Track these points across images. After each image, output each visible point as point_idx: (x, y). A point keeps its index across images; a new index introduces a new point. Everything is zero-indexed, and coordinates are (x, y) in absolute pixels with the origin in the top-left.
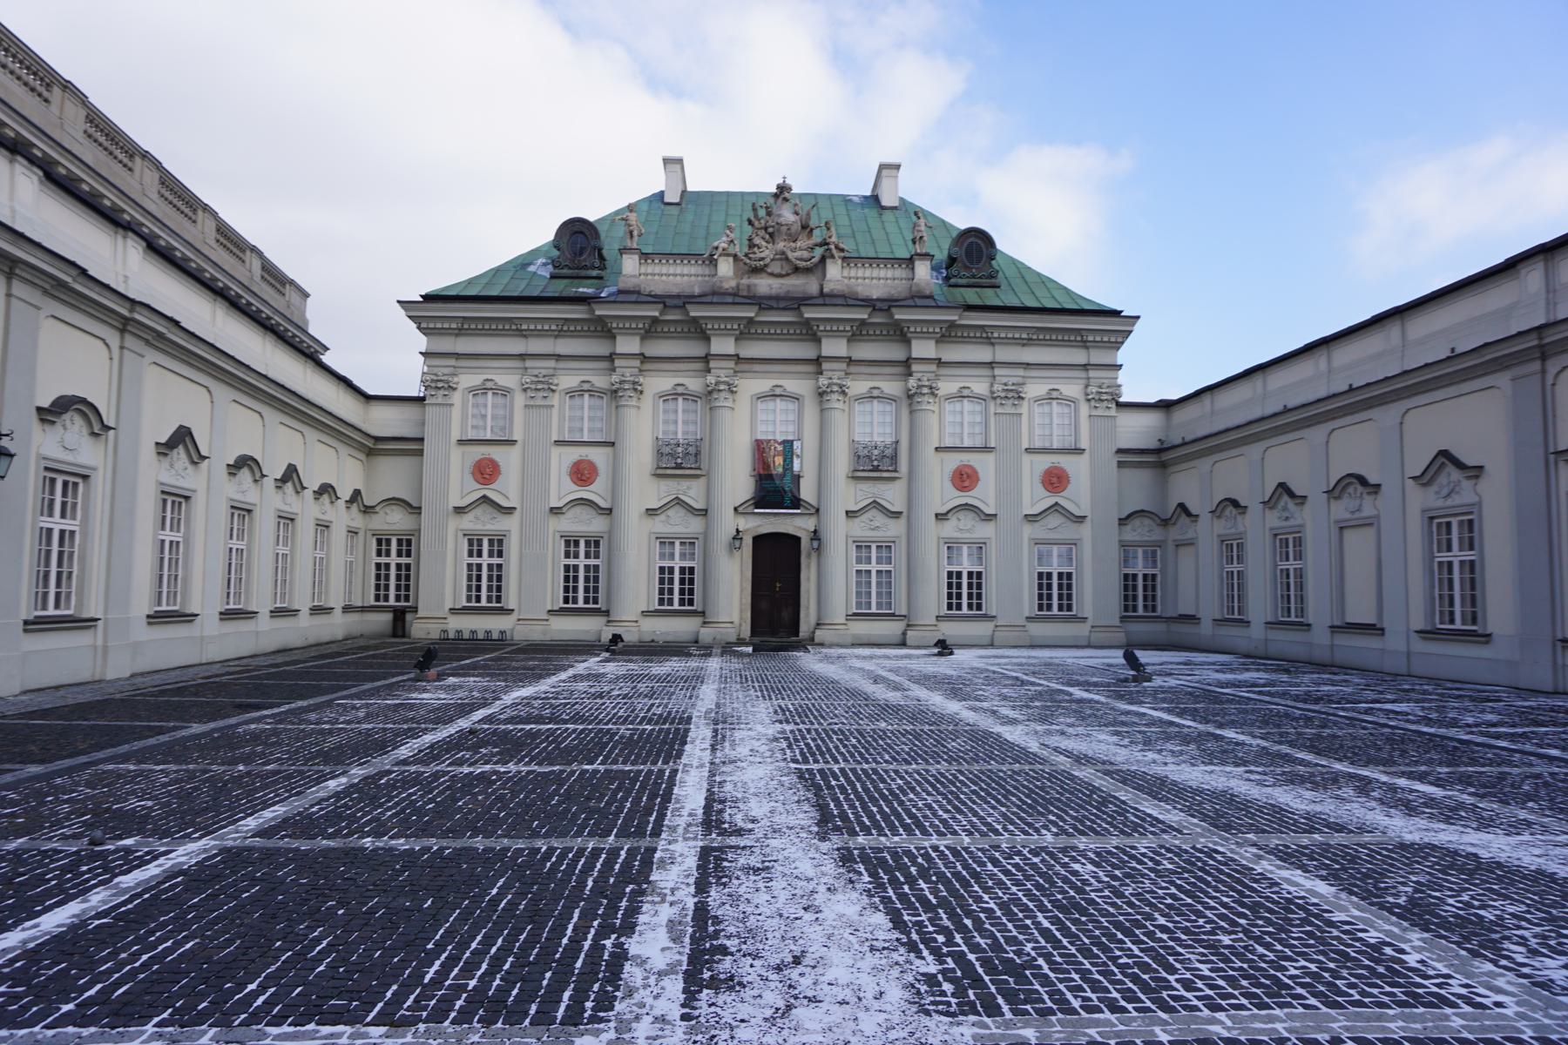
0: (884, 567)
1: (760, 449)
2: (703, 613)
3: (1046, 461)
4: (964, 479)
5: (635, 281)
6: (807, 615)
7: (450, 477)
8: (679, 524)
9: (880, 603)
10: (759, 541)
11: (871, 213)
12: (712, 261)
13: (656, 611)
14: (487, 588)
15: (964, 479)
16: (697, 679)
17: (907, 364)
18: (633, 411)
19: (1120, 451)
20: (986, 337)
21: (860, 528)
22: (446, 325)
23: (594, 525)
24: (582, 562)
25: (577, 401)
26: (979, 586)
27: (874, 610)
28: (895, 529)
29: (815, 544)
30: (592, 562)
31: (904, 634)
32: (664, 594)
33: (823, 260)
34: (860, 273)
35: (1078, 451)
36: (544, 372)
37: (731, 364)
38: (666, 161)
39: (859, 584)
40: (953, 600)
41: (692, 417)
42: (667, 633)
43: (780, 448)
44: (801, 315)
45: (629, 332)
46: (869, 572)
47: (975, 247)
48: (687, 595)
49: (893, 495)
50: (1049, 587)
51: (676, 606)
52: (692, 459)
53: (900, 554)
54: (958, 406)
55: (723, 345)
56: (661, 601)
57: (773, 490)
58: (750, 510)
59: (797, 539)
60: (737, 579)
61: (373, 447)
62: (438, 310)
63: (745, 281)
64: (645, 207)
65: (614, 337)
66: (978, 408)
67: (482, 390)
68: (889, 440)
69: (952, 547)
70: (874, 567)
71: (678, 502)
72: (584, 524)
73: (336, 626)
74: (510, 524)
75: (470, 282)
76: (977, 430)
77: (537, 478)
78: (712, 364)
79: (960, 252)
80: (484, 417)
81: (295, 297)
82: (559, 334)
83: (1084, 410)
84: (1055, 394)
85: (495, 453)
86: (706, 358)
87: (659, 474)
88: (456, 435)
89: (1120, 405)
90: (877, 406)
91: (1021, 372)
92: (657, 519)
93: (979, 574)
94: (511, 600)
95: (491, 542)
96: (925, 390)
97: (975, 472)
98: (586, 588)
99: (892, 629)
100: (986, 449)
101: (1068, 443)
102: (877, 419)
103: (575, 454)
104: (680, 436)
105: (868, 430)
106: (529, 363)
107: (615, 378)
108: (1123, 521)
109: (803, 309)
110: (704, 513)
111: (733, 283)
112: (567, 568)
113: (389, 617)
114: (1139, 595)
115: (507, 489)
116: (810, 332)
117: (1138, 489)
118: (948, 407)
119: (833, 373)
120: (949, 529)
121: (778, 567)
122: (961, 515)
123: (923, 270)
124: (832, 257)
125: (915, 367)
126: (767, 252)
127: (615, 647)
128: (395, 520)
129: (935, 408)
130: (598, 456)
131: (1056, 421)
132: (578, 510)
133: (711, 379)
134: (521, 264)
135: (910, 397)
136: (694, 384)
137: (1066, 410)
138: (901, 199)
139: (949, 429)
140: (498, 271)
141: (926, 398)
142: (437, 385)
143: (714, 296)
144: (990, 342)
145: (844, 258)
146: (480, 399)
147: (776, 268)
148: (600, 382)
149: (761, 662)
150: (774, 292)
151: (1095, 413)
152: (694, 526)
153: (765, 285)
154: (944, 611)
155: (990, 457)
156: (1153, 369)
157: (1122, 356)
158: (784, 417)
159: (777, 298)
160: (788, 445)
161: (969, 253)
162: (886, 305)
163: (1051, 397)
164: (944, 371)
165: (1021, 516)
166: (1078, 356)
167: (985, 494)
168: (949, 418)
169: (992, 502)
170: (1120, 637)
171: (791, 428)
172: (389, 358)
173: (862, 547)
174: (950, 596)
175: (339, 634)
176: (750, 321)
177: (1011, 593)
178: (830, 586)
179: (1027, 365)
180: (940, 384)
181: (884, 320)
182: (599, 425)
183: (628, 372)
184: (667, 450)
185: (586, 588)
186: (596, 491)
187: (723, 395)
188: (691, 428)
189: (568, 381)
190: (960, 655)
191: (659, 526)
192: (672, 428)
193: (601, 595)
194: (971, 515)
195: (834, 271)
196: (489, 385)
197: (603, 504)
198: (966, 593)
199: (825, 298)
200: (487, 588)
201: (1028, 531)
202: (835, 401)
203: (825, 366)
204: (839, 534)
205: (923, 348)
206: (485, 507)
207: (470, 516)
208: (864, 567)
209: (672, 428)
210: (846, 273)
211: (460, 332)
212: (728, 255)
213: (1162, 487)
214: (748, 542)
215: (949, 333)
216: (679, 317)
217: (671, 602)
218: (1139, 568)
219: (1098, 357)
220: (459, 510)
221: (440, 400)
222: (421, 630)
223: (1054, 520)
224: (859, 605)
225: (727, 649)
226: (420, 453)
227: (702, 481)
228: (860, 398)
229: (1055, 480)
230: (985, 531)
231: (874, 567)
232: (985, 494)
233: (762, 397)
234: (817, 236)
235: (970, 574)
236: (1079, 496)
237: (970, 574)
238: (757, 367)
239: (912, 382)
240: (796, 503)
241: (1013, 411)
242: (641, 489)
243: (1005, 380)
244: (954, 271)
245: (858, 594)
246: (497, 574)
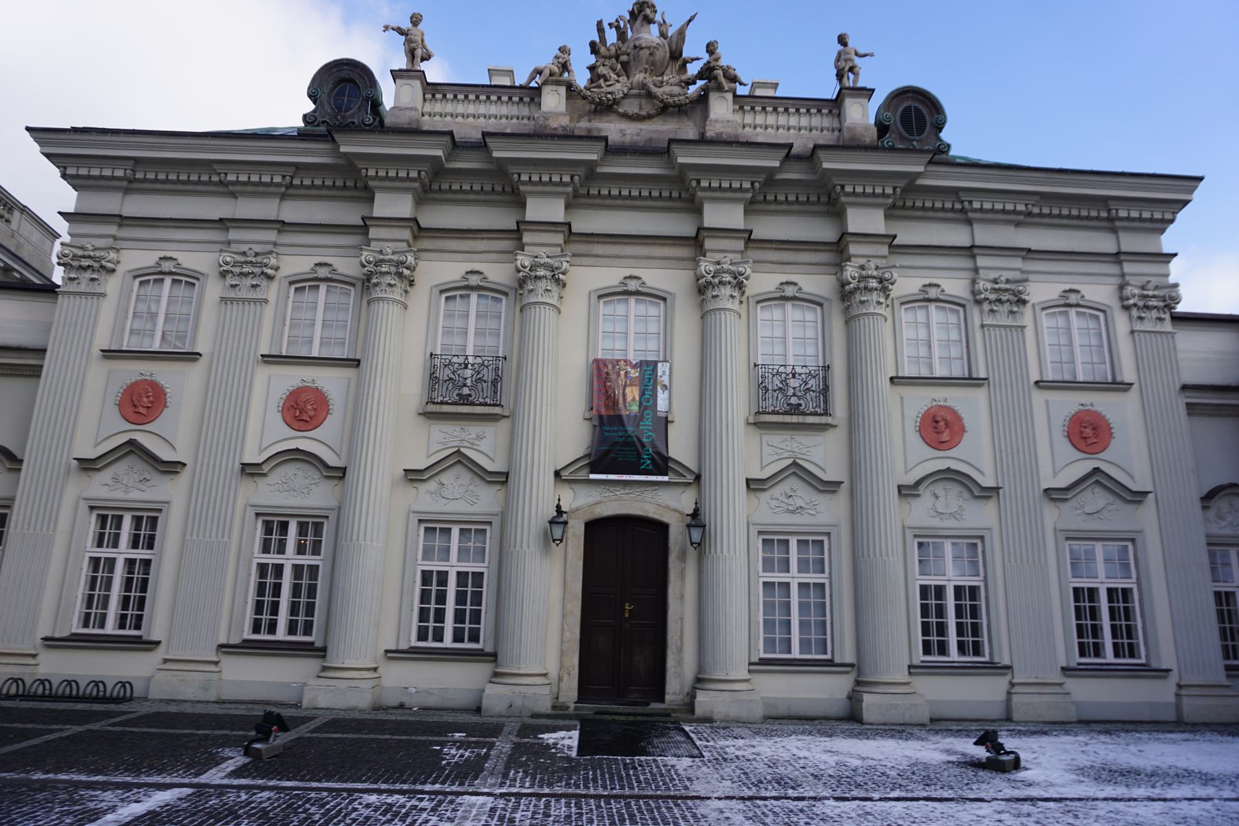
0: (812, 578)
1: (602, 376)
2: (493, 657)
3: (1071, 403)
4: (940, 428)
5: (413, 114)
6: (680, 662)
8: (459, 497)
10: (595, 528)
13: (413, 651)
15: (940, 428)
17: (839, 248)
18: (395, 310)
19: (1185, 388)
21: (770, 510)
22: (107, 172)
23: (311, 495)
25: (307, 296)
26: (975, 612)
27: (796, 654)
28: (828, 512)
29: (696, 535)
30: (307, 560)
31: (854, 698)
32: (430, 615)
33: (702, 100)
34: (760, 119)
35: (1118, 386)
36: (257, 248)
37: (559, 239)
39: (768, 606)
40: (933, 641)
41: (492, 324)
42: (429, 693)
43: (634, 373)
44: (671, 162)
45: (395, 185)
46: (786, 586)
48: (469, 617)
49: (824, 453)
50: (1094, 613)
51: (448, 642)
52: (488, 392)
54: (921, 316)
56: (422, 635)
57: (621, 446)
58: (582, 475)
59: (663, 528)
60: (556, 593)
63: (583, 124)
65: (371, 200)
66: (952, 319)
67: (151, 277)
68: (811, 362)
69: (926, 542)
70: (794, 577)
71: (459, 459)
72: (295, 492)
76: (955, 351)
78: (527, 238)
79: (894, 119)
80: (153, 316)
81: (27, 228)
82: (287, 192)
83: (1121, 324)
84: (1073, 298)
85: (162, 373)
88: (103, 340)
90: (793, 312)
91: (1018, 263)
92: (423, 488)
93: (974, 591)
94: (157, 625)
95: (138, 521)
96: (873, 284)
97: (959, 419)
99: (825, 690)
100: (970, 381)
101: (1103, 372)
102: (793, 332)
103: (294, 377)
104: (470, 352)
105: (778, 350)
106: (233, 235)
107: (366, 255)
109: (676, 149)
110: (502, 479)
111: (565, 121)
112: (263, 568)
115: (172, 434)
116: (683, 193)
118: (905, 316)
120: (921, 512)
121: (628, 574)
122: (939, 489)
124: (720, 88)
125: (853, 249)
126: (619, 87)
129: (887, 313)
130: (330, 381)
131: (1077, 341)
132: (290, 470)
133: (524, 260)
135: (845, 294)
136: (498, 272)
137: (1092, 324)
139: (907, 351)
141: (875, 296)
144: (965, 217)
145: (735, 96)
146: (150, 289)
147: (631, 107)
150: (628, 139)
151: (1138, 326)
152: (485, 500)
153: (614, 129)
154: (919, 657)
157: (1168, 241)
158: (641, 329)
160: (648, 369)
161: (906, 117)
163: (1067, 303)
164: (900, 260)
165: (1038, 494)
166: (1103, 242)
167: (976, 453)
168: (907, 333)
169: (987, 465)
171: (652, 345)
173: (774, 542)
174: (926, 629)
176: (590, 165)
179: (1028, 253)
180: (895, 275)
182: (340, 334)
183: (388, 248)
184: (445, 374)
186: (322, 441)
187: (542, 285)
188: (490, 341)
191: (427, 499)
192: (458, 340)
193: (317, 619)
194: (955, 489)
195: (721, 109)
196: (167, 266)
197: (332, 460)
198: (955, 625)
201: (1052, 516)
203: (709, 244)
204: (737, 518)
206: (131, 461)
207: (106, 476)
208: (777, 577)
209: (458, 340)
210: (738, 118)
211: (130, 186)
212: (558, 83)
214: (577, 530)
215: (906, 201)
217: (439, 636)
219: (1130, 242)
220: (88, 465)
221: (83, 288)
223: (1095, 499)
224: (769, 644)
226: (35, 372)
227: (504, 425)
228: (763, 300)
229: (1088, 432)
230: (981, 516)
231: (794, 577)
232: (976, 453)
233: (605, 295)
235: (958, 590)
236: (1129, 456)
237: (958, 590)
238: (599, 249)
239: (850, 271)
240: (662, 464)
241: (1009, 321)
242: (393, 430)
243: (993, 275)
244: (887, 141)
245: (769, 624)
246: (139, 579)
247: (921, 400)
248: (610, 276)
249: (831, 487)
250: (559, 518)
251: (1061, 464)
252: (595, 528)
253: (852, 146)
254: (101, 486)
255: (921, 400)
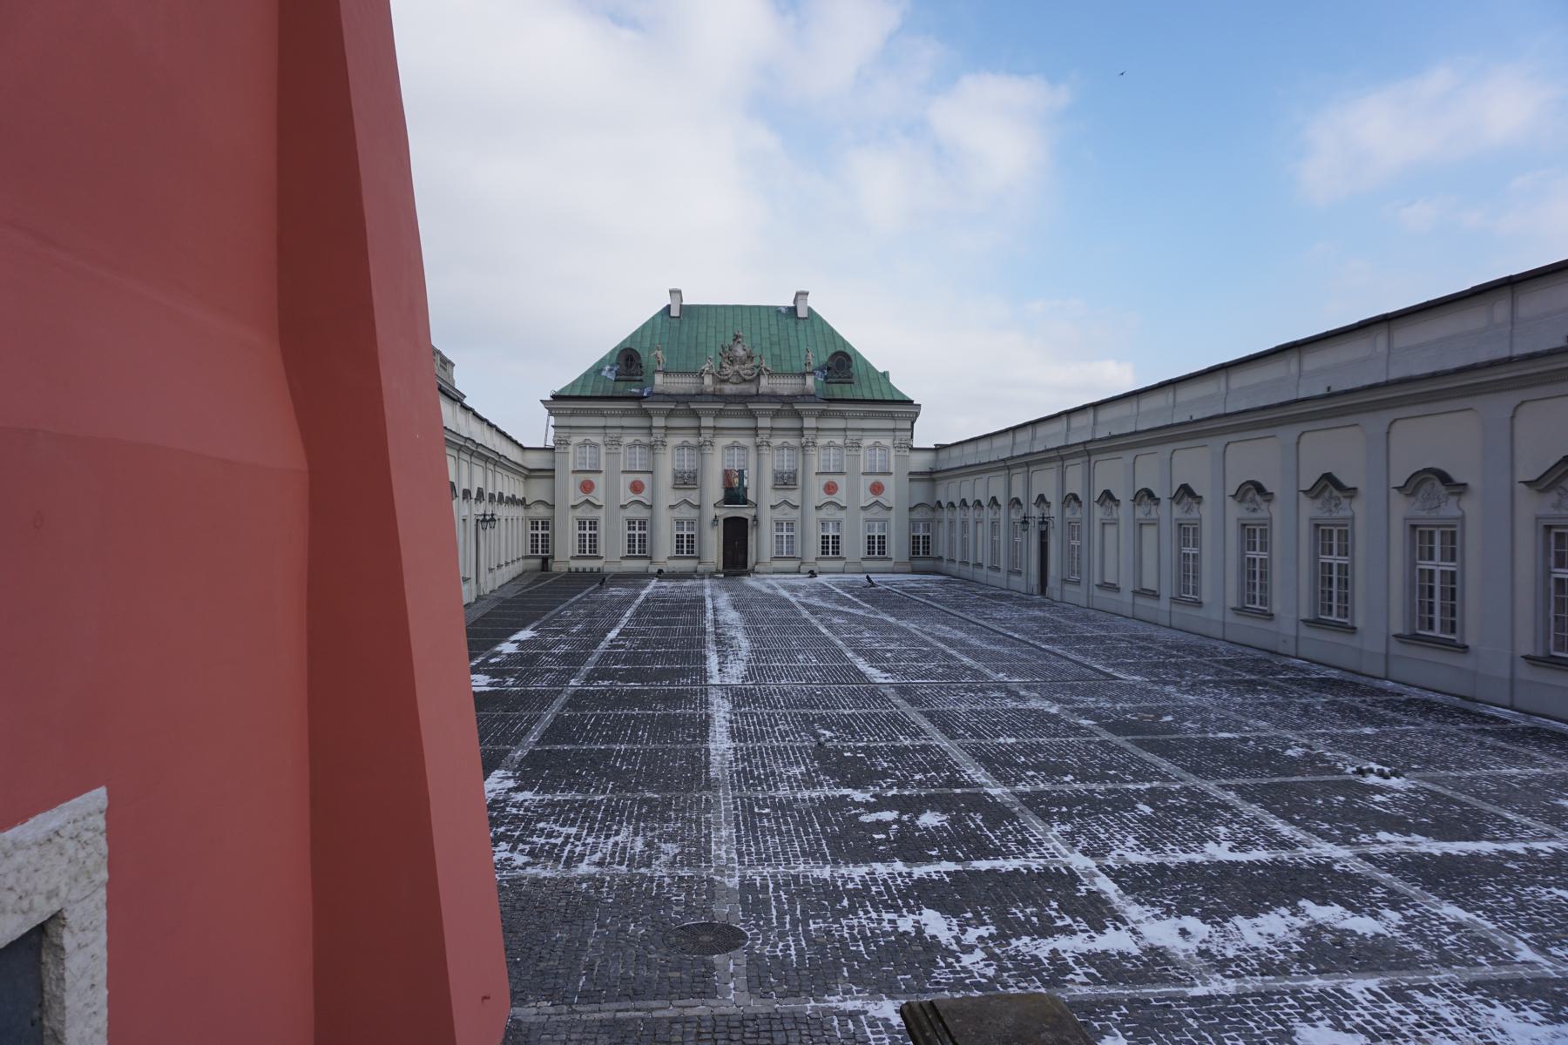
1: (727, 474)
3: (873, 479)
4: (830, 488)
7: (570, 491)
8: (686, 513)
9: (788, 553)
10: (726, 521)
11: (791, 322)
12: (701, 375)
14: (589, 546)
15: (830, 488)
16: (702, 588)
17: (801, 431)
20: (842, 415)
23: (643, 514)
24: (637, 532)
28: (795, 514)
32: (679, 547)
38: (671, 292)
45: (659, 415)
47: (842, 363)
49: (794, 497)
53: (797, 527)
55: (707, 422)
57: (734, 494)
61: (530, 474)
62: (559, 402)
64: (659, 320)
67: (584, 444)
70: (785, 533)
71: (686, 501)
73: (517, 568)
74: (600, 514)
75: (573, 384)
77: (613, 491)
82: (623, 416)
86: (699, 428)
87: (676, 487)
88: (571, 468)
89: (912, 449)
98: (640, 545)
100: (841, 473)
103: (632, 478)
108: (911, 509)
110: (699, 507)
113: (539, 561)
114: (920, 548)
115: (598, 496)
116: (752, 415)
117: (920, 492)
119: (763, 435)
120: (823, 514)
121: (736, 534)
123: (810, 380)
126: (729, 370)
127: (660, 574)
128: (541, 512)
130: (644, 478)
134: (597, 370)
136: (693, 441)
138: (810, 309)
140: (586, 375)
142: (561, 442)
143: (700, 396)
147: (734, 379)
148: (645, 440)
149: (730, 582)
152: (694, 514)
153: (728, 389)
155: (843, 478)
156: (927, 433)
159: (735, 396)
162: (791, 399)
163: (875, 446)
166: (889, 424)
167: (841, 497)
170: (909, 568)
172: (535, 429)
173: (779, 524)
175: (520, 571)
177: (853, 546)
178: (763, 543)
181: (788, 405)
185: (640, 545)
186: (644, 496)
189: (628, 439)
190: (821, 579)
191: (677, 514)
195: (764, 381)
198: (831, 546)
199: (758, 397)
200: (589, 546)
201: (863, 514)
202: (765, 451)
204: (767, 517)
205: (809, 422)
211: (572, 415)
213: (933, 492)
215: (822, 415)
216: (684, 404)
218: (921, 533)
220: (574, 507)
222: (556, 567)
223: (876, 509)
225: (712, 575)
229: (877, 489)
230: (841, 515)
231: (785, 533)
232: (841, 497)
233: (728, 447)
234: (756, 362)
236: (889, 497)
240: (745, 501)
242: (667, 496)
246: (593, 538)
247: (825, 479)
248: (728, 441)
249: (796, 507)
250: (716, 519)
251: (866, 498)
252: (726, 521)
253: (805, 397)
254: (579, 513)
255: (825, 479)
